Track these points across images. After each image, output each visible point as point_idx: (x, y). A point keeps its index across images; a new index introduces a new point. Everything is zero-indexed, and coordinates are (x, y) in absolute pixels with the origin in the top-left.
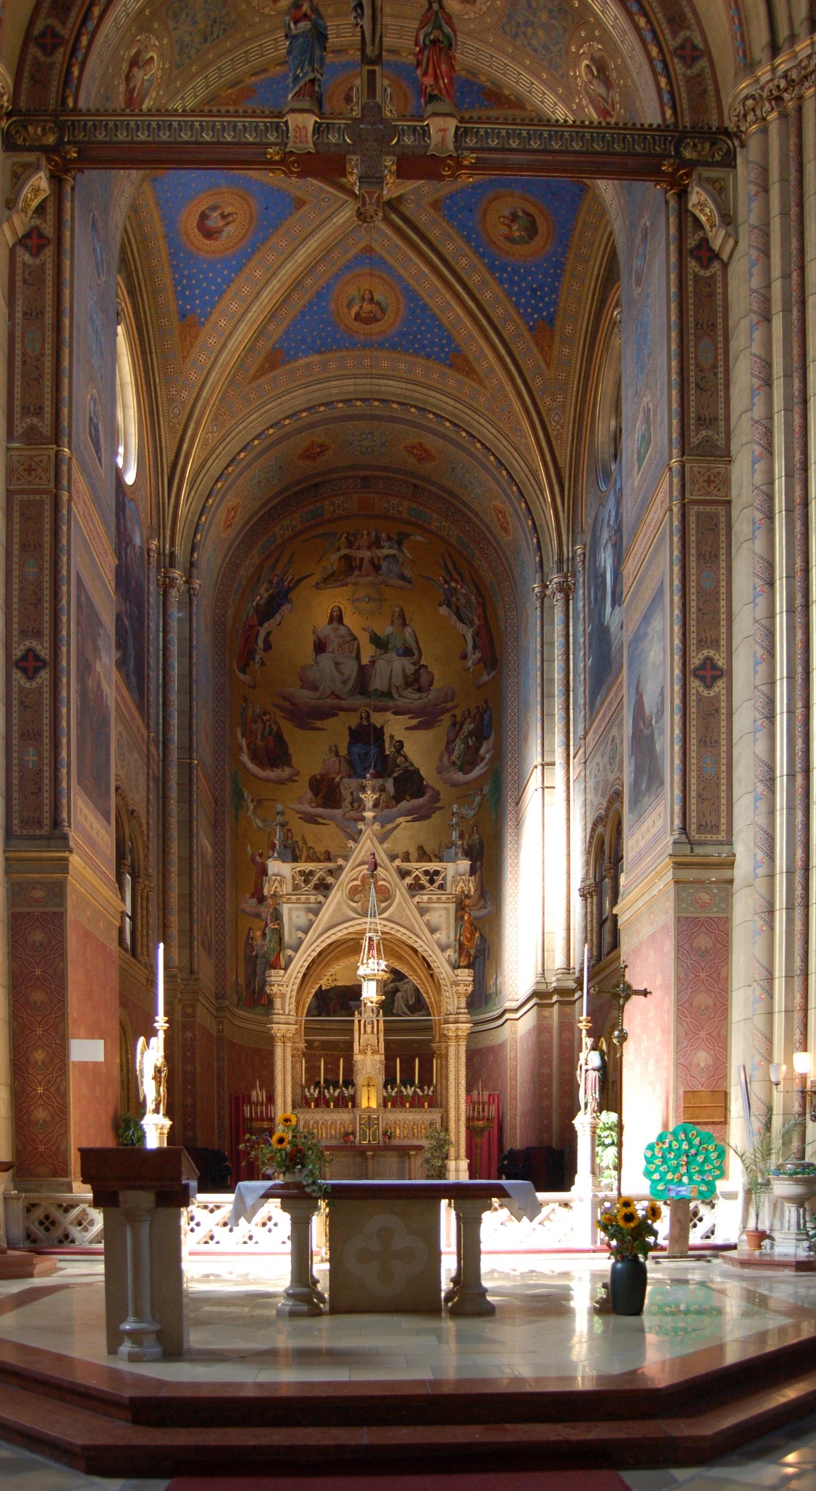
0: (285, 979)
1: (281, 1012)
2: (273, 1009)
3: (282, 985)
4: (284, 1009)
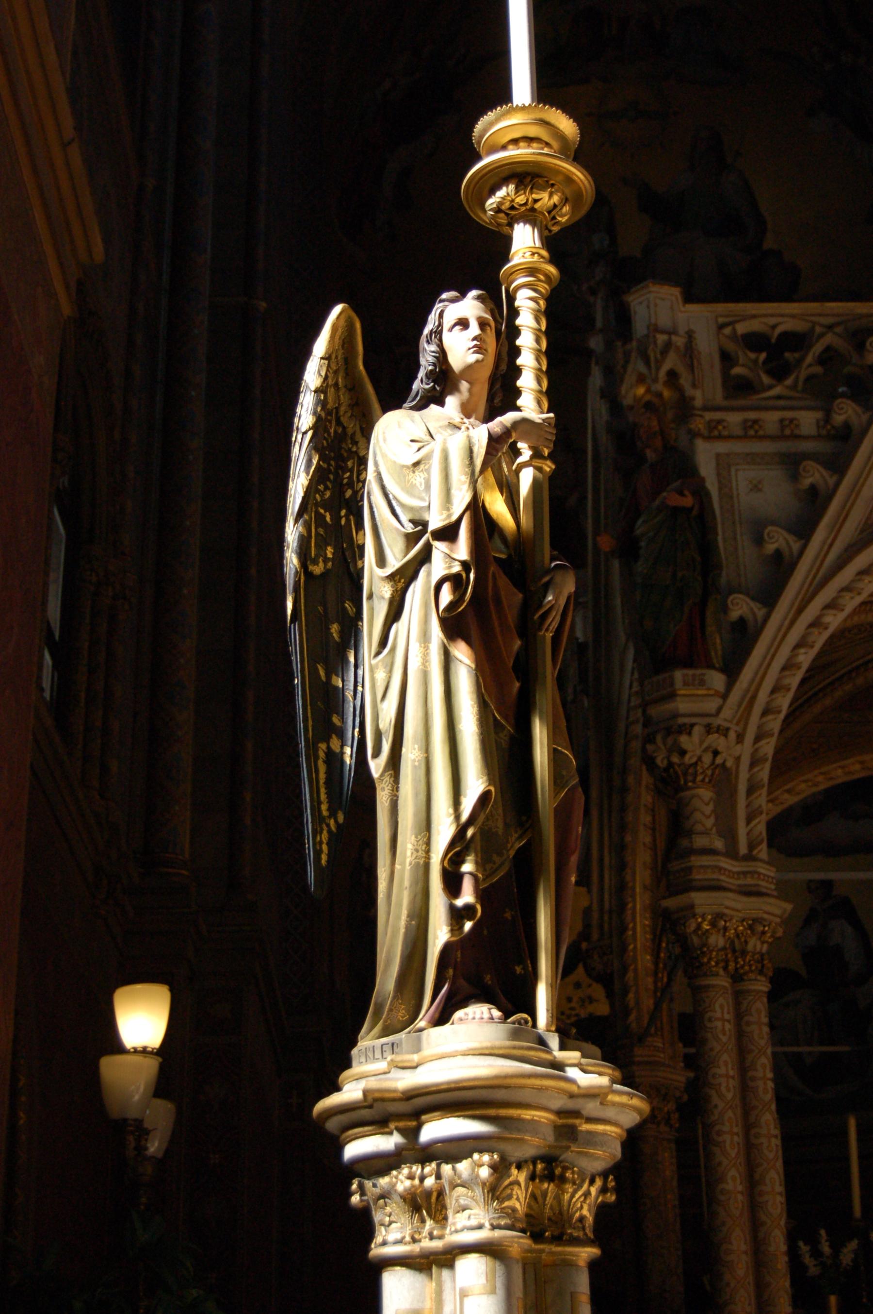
0: (726, 713)
1: (719, 844)
2: (690, 833)
3: (724, 732)
4: (730, 835)
